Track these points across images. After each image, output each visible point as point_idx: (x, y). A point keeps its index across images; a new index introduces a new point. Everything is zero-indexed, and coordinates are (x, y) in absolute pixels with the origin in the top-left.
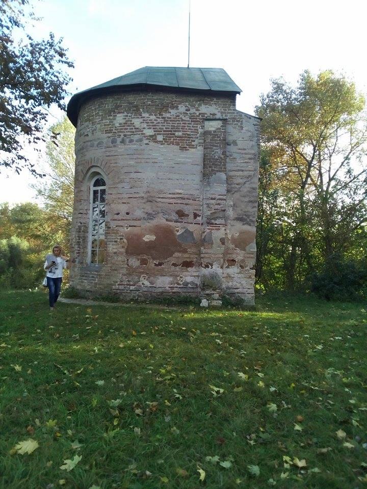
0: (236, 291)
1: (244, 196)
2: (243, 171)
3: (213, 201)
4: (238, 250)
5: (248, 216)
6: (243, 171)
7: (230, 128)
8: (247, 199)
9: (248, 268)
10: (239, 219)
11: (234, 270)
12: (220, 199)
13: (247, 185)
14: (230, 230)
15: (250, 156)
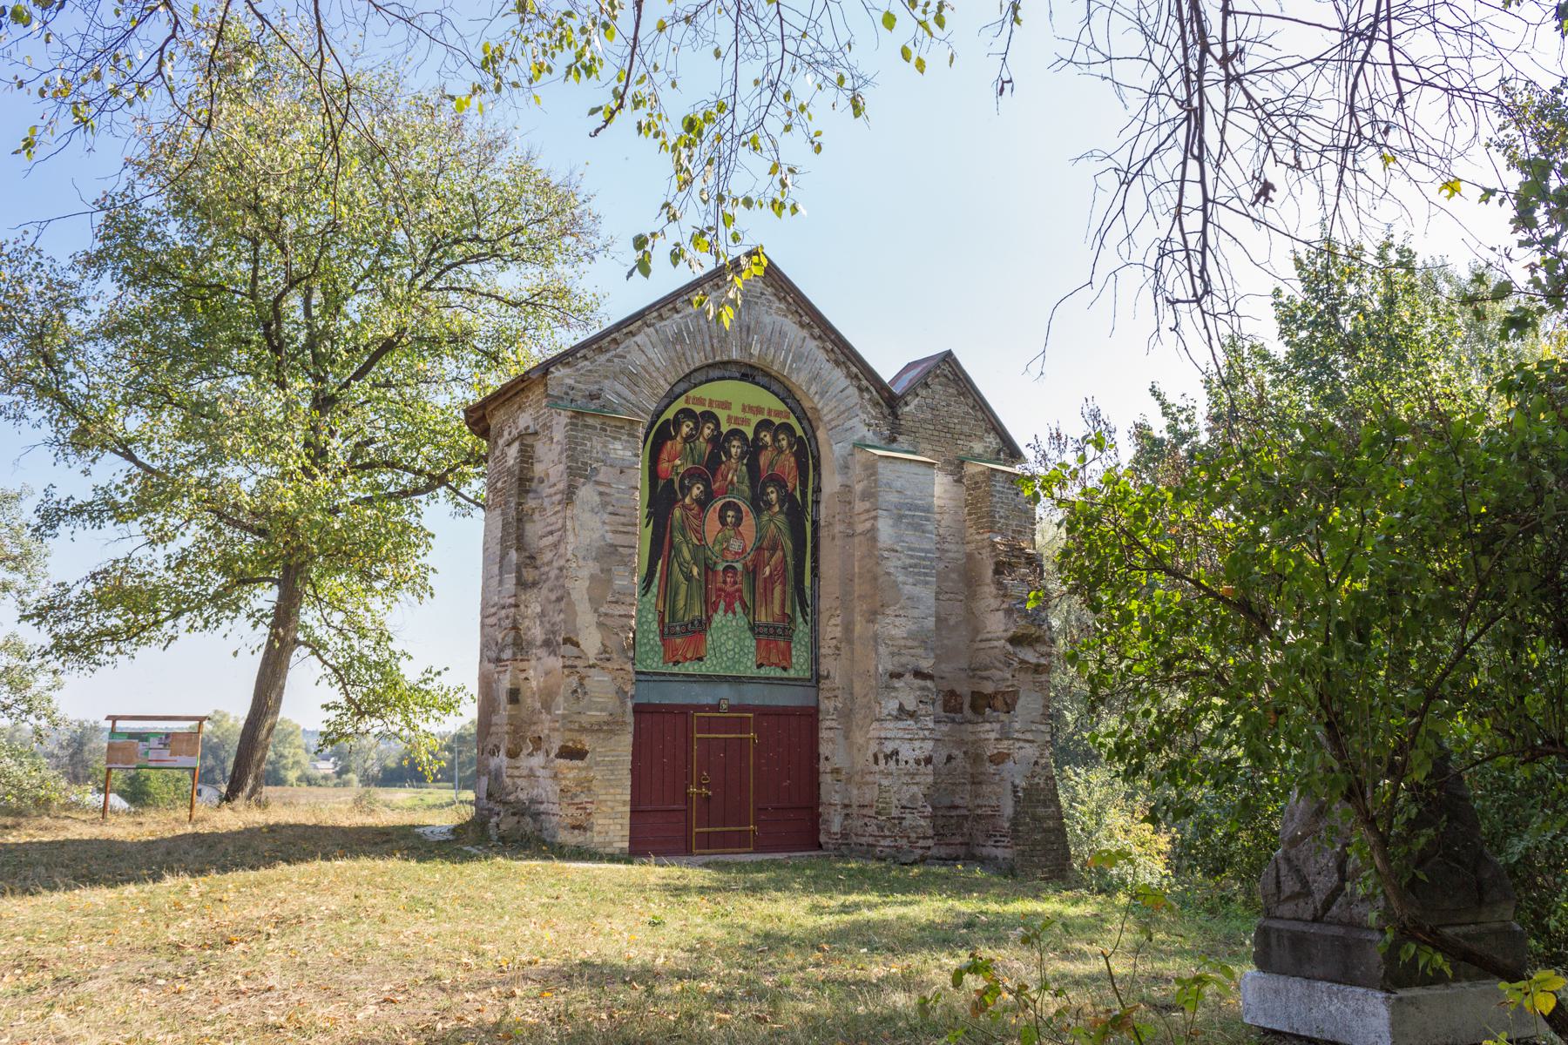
0: (542, 808)
1: (551, 590)
2: (551, 533)
3: (503, 613)
4: (544, 716)
5: (554, 633)
6: (551, 533)
7: (541, 448)
8: (553, 597)
9: (552, 755)
10: (547, 643)
11: (538, 760)
12: (510, 606)
13: (555, 564)
14: (535, 669)
15: (558, 497)
